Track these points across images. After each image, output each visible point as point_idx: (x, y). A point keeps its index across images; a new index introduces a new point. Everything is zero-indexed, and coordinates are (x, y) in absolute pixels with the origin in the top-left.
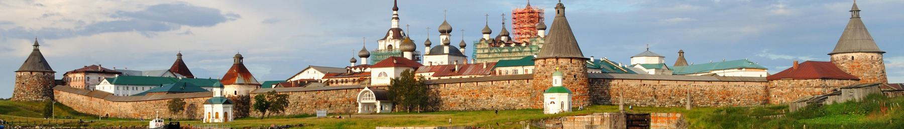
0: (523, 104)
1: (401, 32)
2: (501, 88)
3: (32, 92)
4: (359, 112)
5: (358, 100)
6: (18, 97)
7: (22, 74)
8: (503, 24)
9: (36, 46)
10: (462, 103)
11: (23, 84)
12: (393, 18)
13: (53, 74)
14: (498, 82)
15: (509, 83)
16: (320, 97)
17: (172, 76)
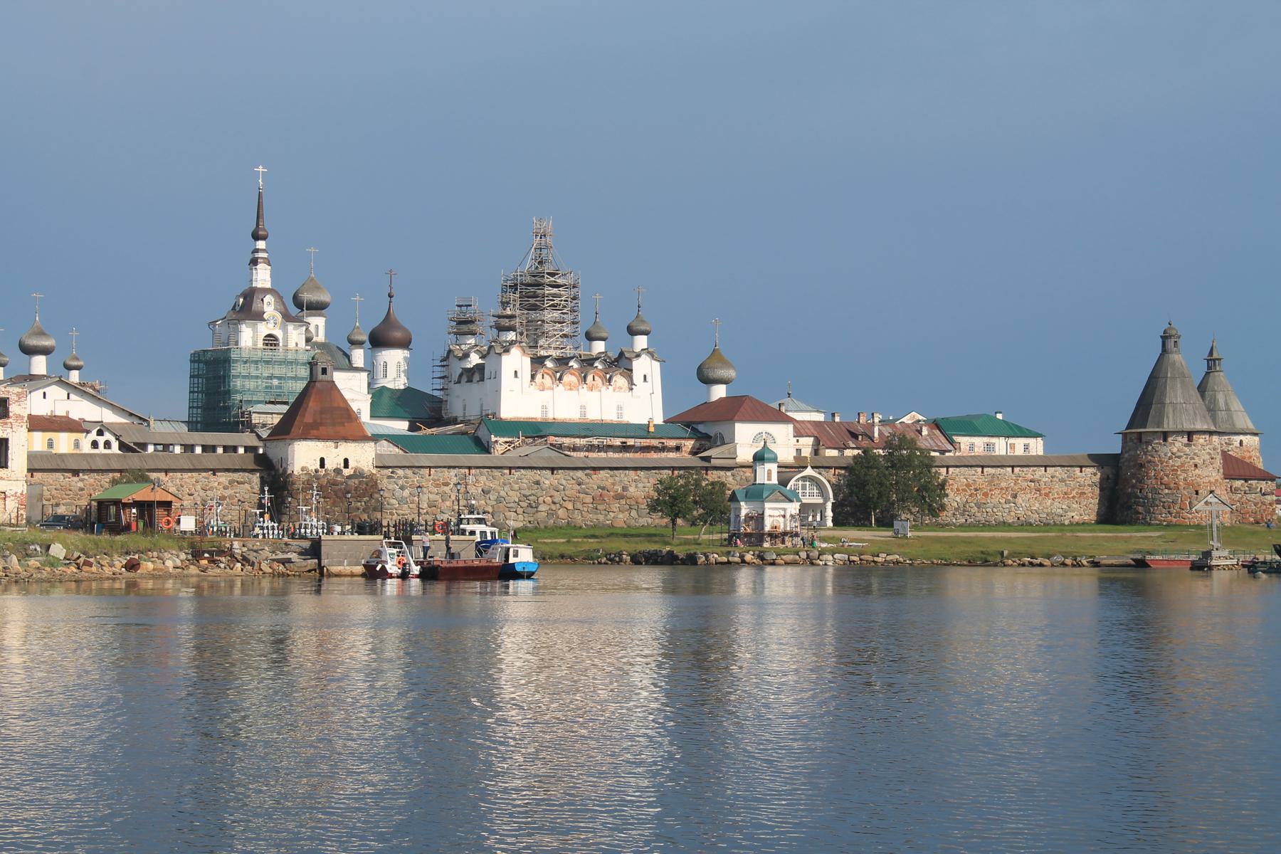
0: (1073, 514)
14: (1025, 469)
15: (1046, 471)
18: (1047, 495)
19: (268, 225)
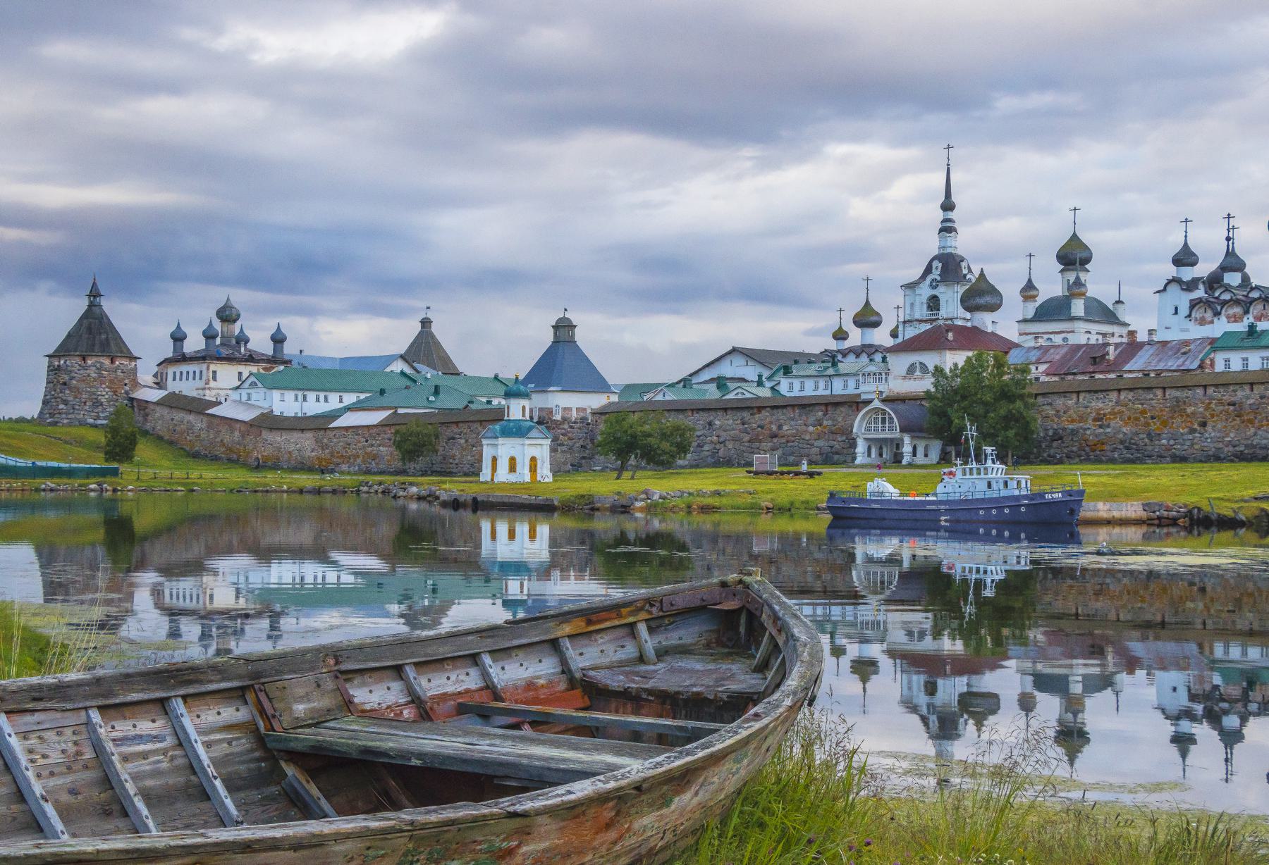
1: (963, 264)
2: (1229, 404)
3: (85, 403)
4: (859, 461)
5: (855, 430)
6: (52, 415)
7: (62, 362)
8: (1228, 239)
9: (95, 297)
10: (1122, 442)
11: (65, 384)
12: (941, 231)
13: (133, 364)
15: (1252, 390)
16: (759, 423)
17: (408, 370)
18: (1250, 421)
19: (954, 198)
